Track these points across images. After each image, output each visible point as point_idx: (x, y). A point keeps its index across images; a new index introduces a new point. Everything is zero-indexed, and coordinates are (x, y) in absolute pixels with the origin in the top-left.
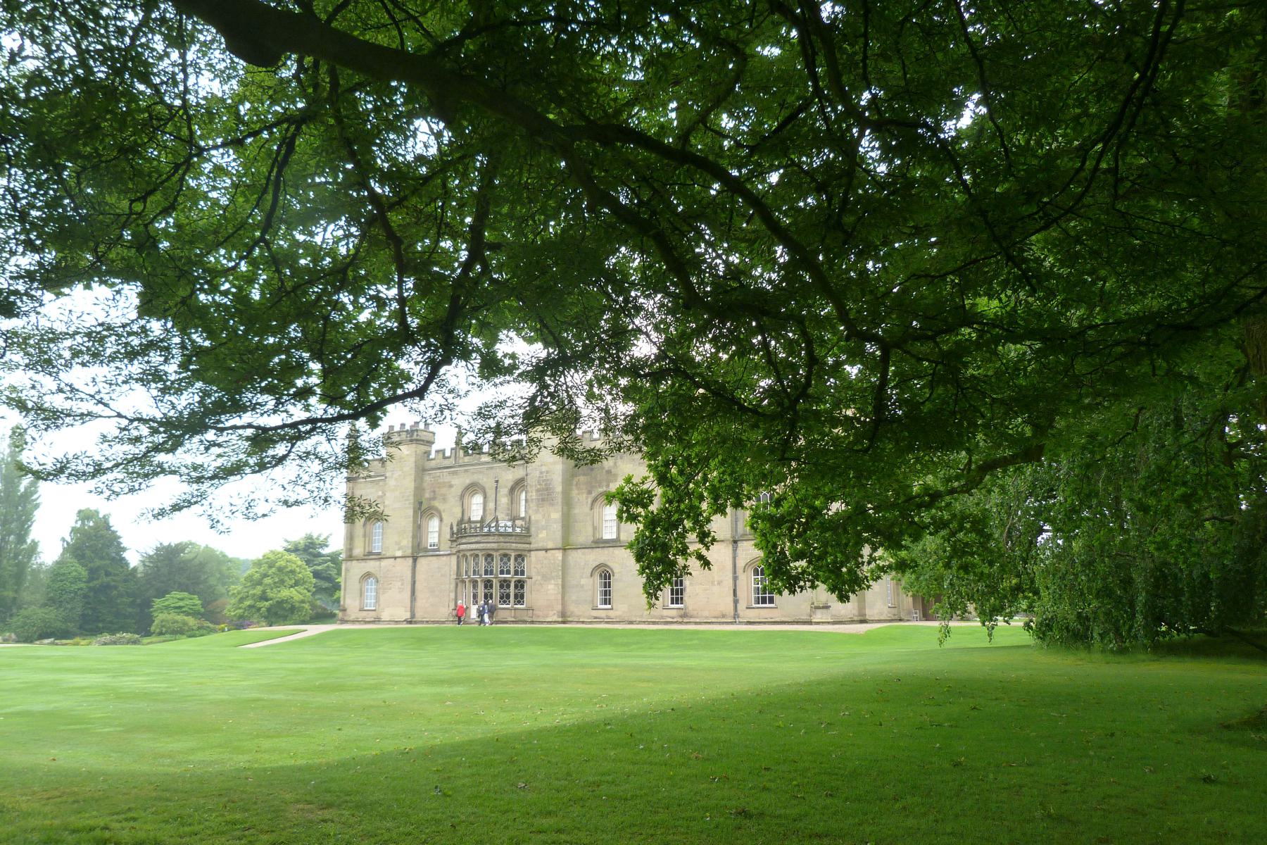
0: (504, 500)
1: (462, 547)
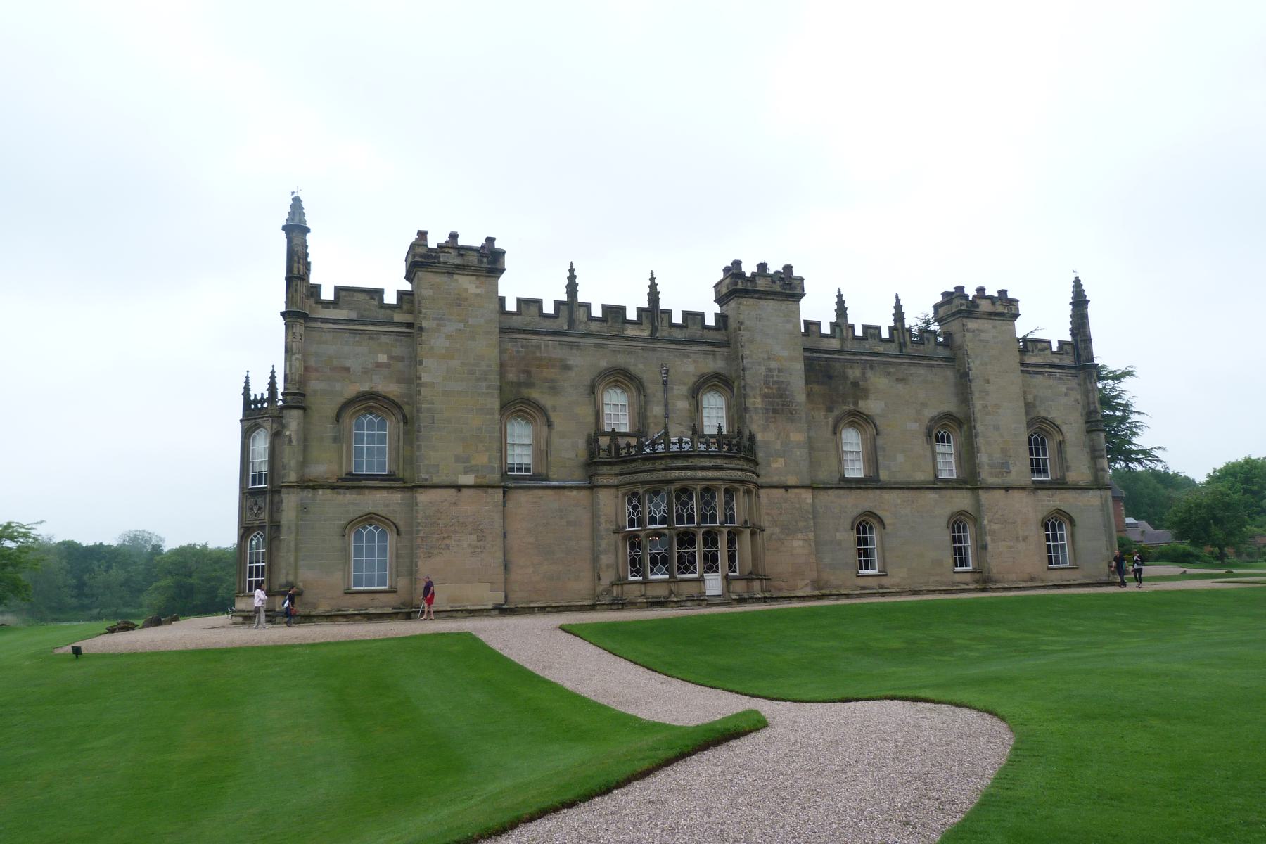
0: (682, 405)
1: (675, 474)
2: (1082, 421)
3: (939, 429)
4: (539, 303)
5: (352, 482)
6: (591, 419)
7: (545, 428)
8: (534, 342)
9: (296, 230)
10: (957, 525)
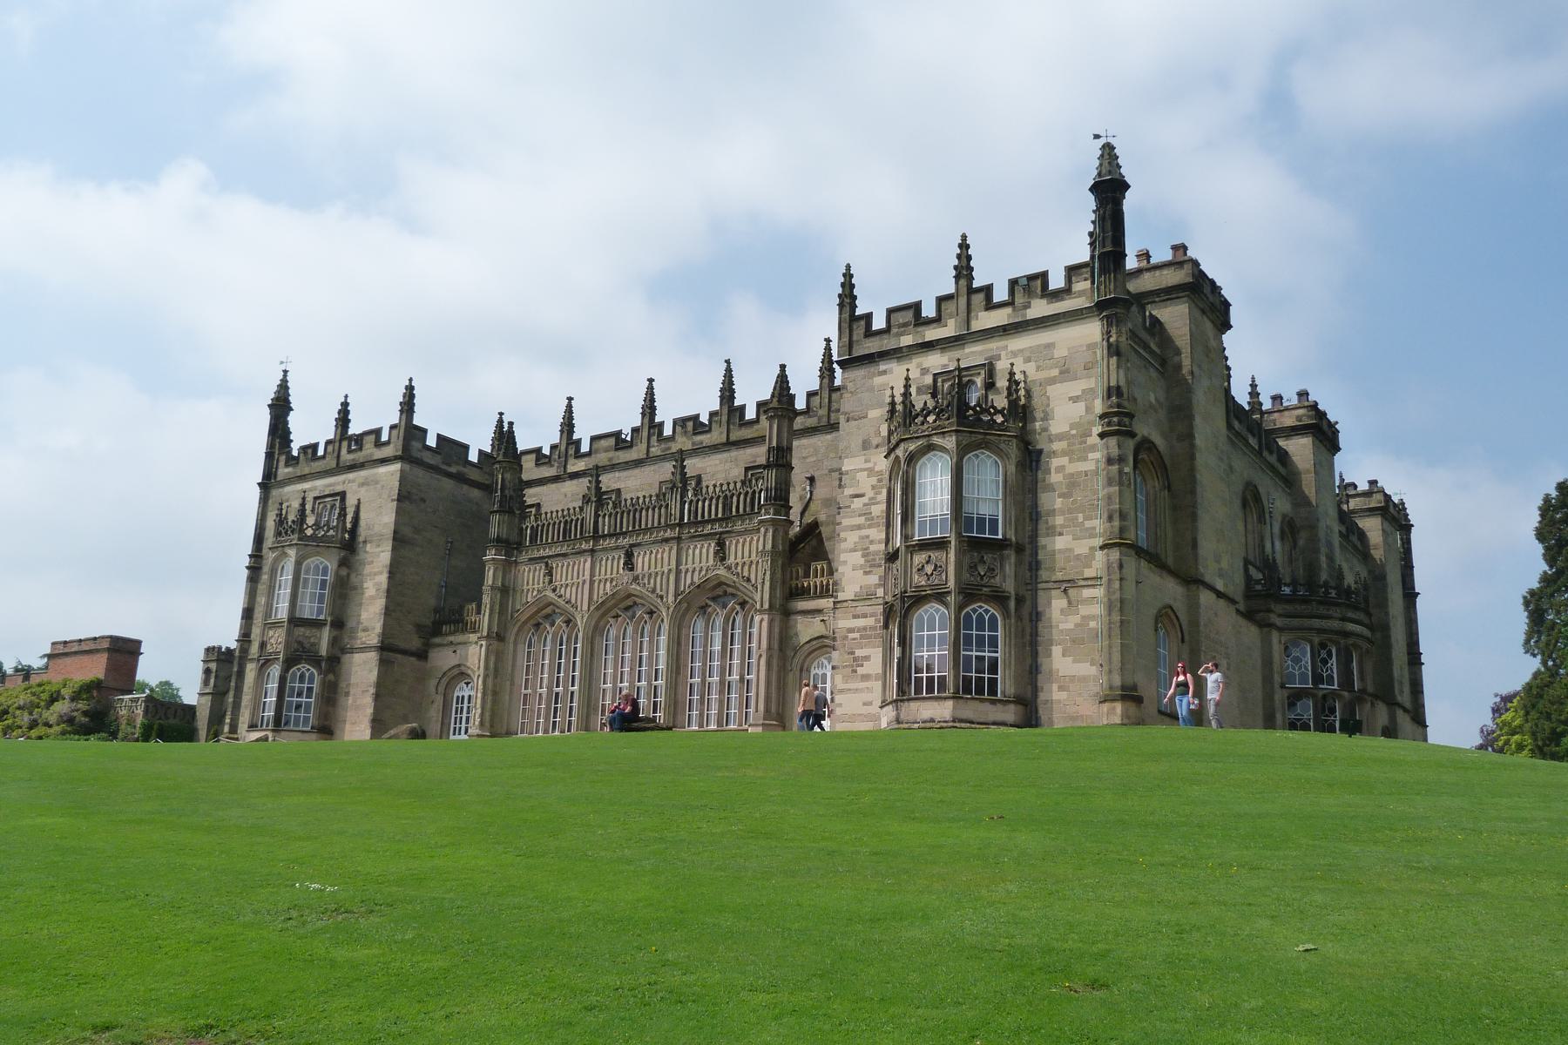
1: (1351, 627)
9: (1110, 191)
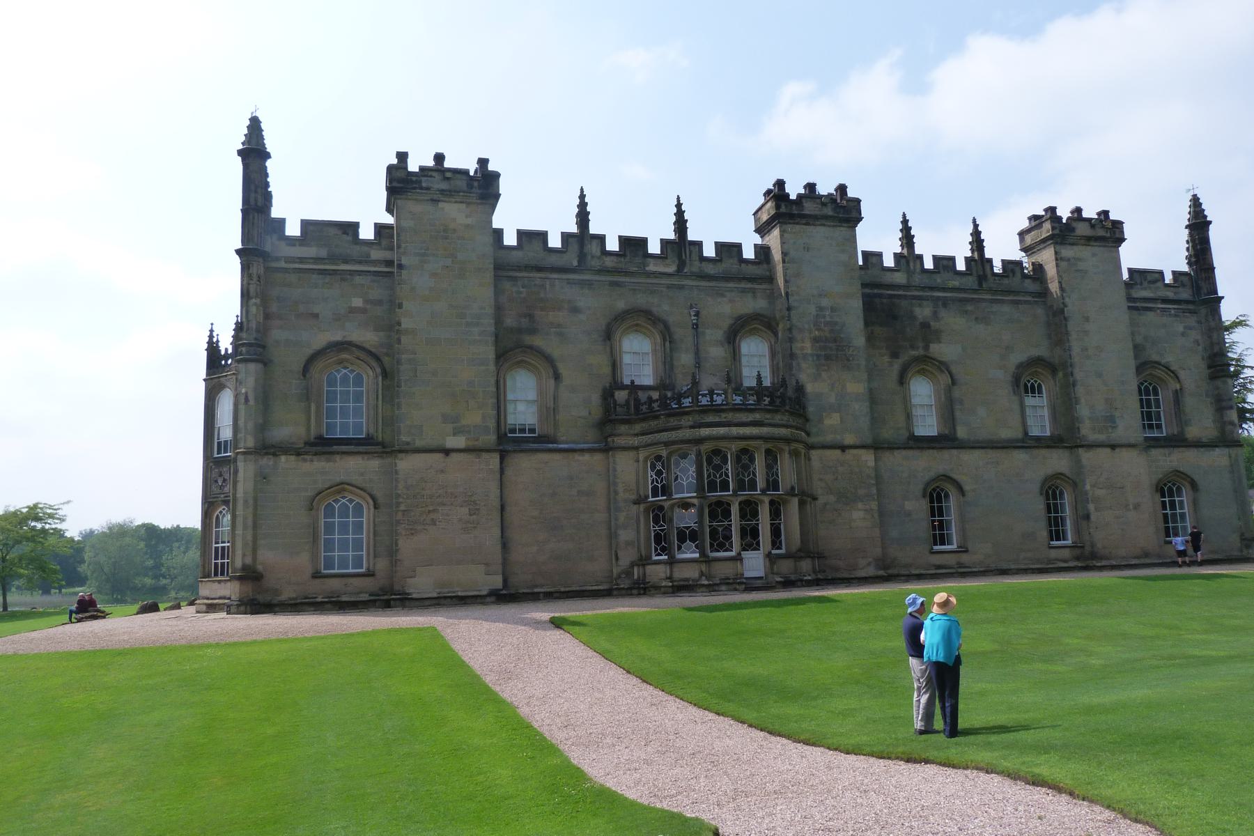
0: (716, 353)
1: (705, 432)
2: (1203, 365)
3: (1024, 381)
4: (543, 236)
5: (323, 445)
6: (607, 370)
7: (552, 382)
8: (538, 282)
9: (254, 153)
10: (1051, 491)
